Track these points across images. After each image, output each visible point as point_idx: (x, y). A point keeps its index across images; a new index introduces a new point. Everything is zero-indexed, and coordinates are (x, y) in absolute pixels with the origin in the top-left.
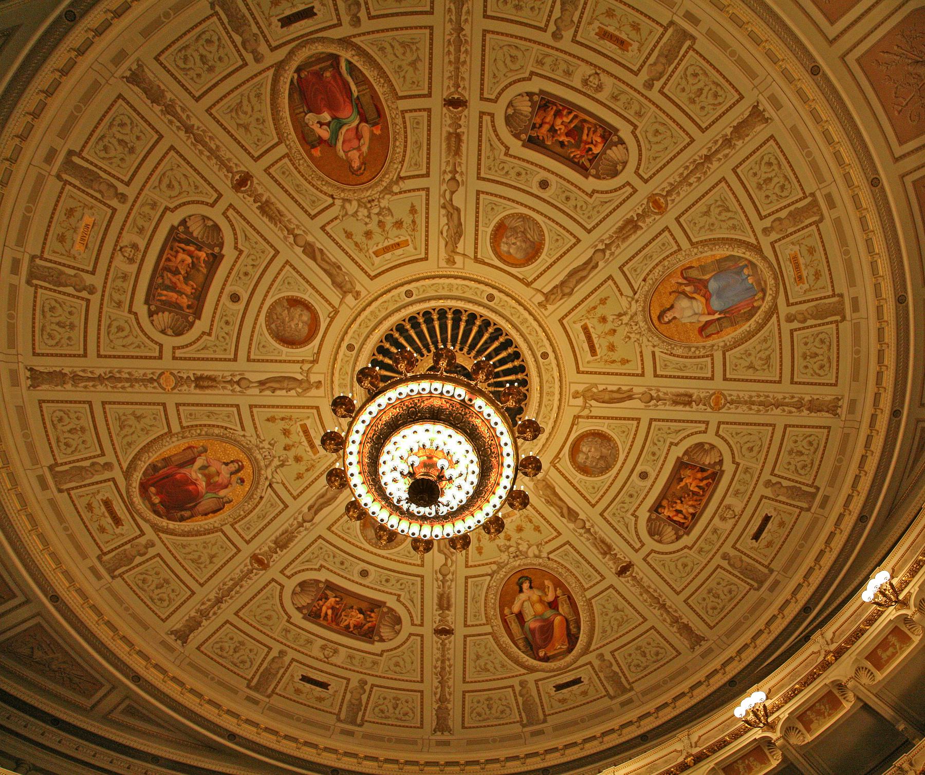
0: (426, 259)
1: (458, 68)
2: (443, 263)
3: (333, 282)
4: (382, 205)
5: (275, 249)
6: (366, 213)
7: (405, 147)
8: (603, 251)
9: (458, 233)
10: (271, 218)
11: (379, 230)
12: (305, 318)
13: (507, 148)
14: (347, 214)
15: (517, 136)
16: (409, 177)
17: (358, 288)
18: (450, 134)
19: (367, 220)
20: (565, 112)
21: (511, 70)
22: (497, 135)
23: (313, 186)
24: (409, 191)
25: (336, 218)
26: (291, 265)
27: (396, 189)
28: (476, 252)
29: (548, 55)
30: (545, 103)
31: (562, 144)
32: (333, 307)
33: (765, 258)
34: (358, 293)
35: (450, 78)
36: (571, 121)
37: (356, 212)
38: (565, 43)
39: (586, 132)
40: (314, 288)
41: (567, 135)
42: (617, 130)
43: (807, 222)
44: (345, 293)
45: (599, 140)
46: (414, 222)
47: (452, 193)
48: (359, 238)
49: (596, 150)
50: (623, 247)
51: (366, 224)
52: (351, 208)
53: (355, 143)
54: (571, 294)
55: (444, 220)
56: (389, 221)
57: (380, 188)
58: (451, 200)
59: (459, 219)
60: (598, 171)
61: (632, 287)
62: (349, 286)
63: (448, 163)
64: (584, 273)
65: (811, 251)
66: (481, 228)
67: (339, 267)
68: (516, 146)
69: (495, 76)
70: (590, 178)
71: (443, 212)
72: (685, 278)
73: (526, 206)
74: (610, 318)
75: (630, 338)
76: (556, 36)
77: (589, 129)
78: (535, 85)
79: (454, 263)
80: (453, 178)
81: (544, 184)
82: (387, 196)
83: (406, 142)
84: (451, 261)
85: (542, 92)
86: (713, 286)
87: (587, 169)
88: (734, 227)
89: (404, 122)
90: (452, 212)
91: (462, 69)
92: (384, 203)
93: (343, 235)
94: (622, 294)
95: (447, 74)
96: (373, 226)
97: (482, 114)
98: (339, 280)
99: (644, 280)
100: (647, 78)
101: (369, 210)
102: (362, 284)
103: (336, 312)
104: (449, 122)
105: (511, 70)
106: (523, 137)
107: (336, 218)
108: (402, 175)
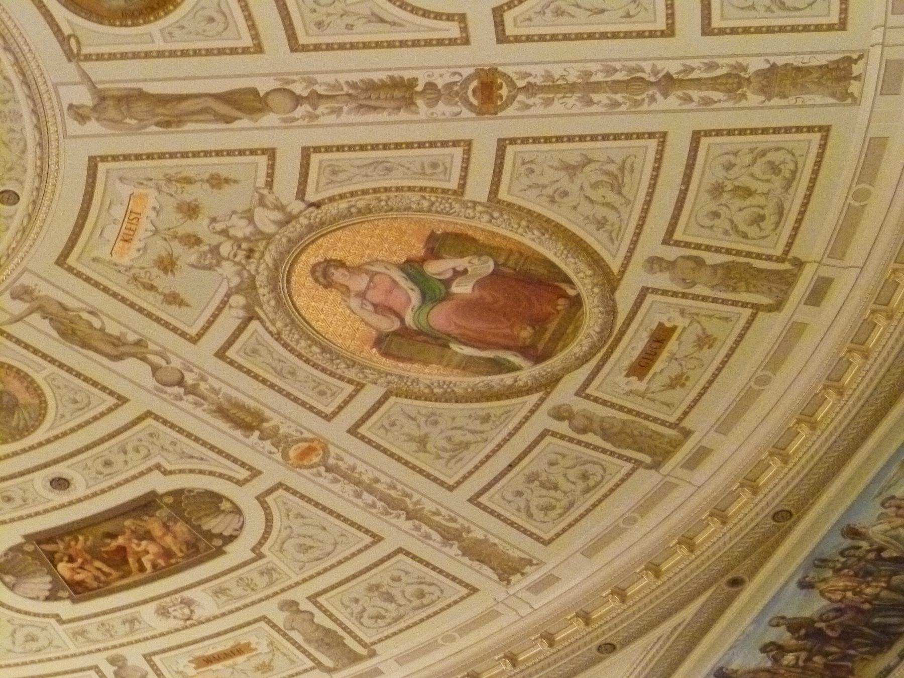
0: (61, 261)
1: (358, 483)
2: (27, 280)
3: (141, 95)
4: (225, 264)
5: (305, 48)
6: (232, 232)
7: (300, 356)
9: (69, 329)
10: (372, 87)
11: (181, 231)
13: (166, 473)
14: (262, 203)
15: (177, 494)
16: (240, 330)
17: (93, 126)
18: (264, 420)
19: (219, 226)
20: (161, 562)
21: (289, 537)
22: (201, 472)
23: (365, 192)
24: (215, 316)
25: (270, 184)
26: (245, 51)
27: (238, 300)
29: (271, 583)
30: (202, 548)
31: (113, 536)
32: (88, 58)
35: (353, 469)
36: (139, 561)
37: (251, 220)
38: (271, 609)
39: (106, 569)
40: (160, 54)
41: (122, 550)
42: (74, 601)
44: (102, 98)
45: (78, 577)
46: (152, 288)
47: (155, 369)
48: (196, 193)
49: (63, 568)
51: (214, 220)
52: (266, 220)
53: (376, 296)
55: (113, 329)
56: (190, 256)
57: (261, 280)
58: (144, 359)
59: (97, 350)
60: (25, 553)
62: (112, 113)
63: (216, 392)
66: (51, 368)
67: (167, 124)
68: (161, 484)
69: (300, 516)
70: (22, 540)
71: (132, 337)
73: (40, 445)
76: (292, 606)
77: (106, 575)
78: (238, 552)
79: (15, 296)
80: (181, 382)
81: (60, 483)
82: (236, 281)
83: (307, 361)
84: (23, 294)
85: (220, 552)
87: (39, 543)
89: (341, 378)
90: (118, 349)
91: (350, 489)
92: (228, 269)
93: (224, 174)
95: (361, 467)
96: (200, 226)
97: (255, 473)
98: (140, 107)
100: (130, 663)
101: (238, 242)
102: (97, 138)
103: (71, 56)
104: (283, 430)
105: (289, 537)
106: (169, 500)
107: (270, 184)
108: (254, 325)
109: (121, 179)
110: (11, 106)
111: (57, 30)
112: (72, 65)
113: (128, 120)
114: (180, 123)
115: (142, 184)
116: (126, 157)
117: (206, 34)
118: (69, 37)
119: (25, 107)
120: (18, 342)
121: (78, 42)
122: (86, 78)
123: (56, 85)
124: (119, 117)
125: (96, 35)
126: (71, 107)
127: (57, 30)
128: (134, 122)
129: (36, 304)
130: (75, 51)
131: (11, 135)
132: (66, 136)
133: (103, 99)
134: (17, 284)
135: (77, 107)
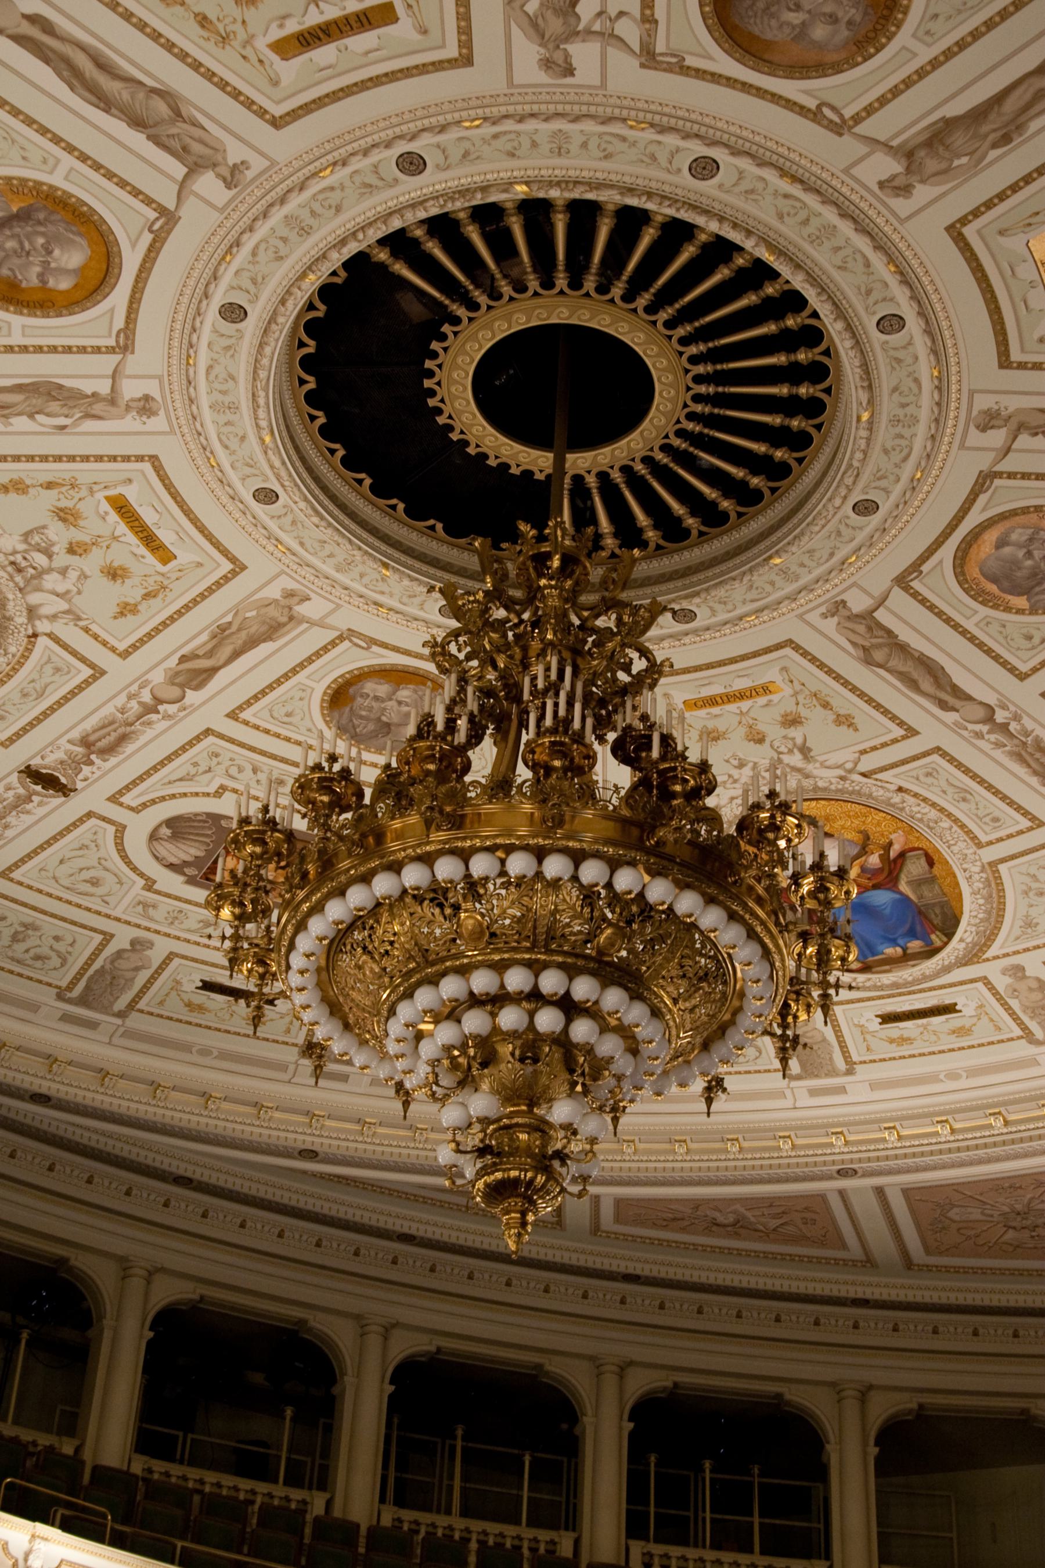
0: (1005, 362)
2: (983, 403)
3: (949, 124)
8: (989, 718)
12: (819, 32)
17: (923, 193)
28: (1011, 475)
32: (857, 119)
33: (947, 969)
34: (905, 190)
40: (935, 64)
43: (1033, 1026)
44: (908, 154)
50: (998, 754)
54: (868, 661)
61: (883, 769)
62: (932, 165)
64: (926, 684)
65: (961, 1032)
67: (1006, 139)
72: (902, 855)
74: (797, 734)
75: (741, 765)
79: (983, 428)
84: (989, 421)
86: (882, 898)
88: (1029, 924)
94: (863, 752)
98: (959, 139)
99: (900, 789)
103: (839, 128)
109: (1001, 233)
110: (815, 222)
111: (801, 110)
112: (846, 137)
113: (956, 163)
114: (1020, 128)
115: (1030, 225)
116: (989, 205)
117: (969, 5)
118: (819, 107)
119: (830, 215)
120: (1025, 476)
121: (833, 108)
122: (873, 142)
123: (846, 171)
124: (944, 165)
125: (848, 88)
126: (881, 185)
127: (801, 110)
128: (964, 160)
129: (1013, 424)
130: (836, 119)
131: (842, 254)
132: (902, 221)
133: (910, 155)
134: (975, 413)
135: (888, 181)
